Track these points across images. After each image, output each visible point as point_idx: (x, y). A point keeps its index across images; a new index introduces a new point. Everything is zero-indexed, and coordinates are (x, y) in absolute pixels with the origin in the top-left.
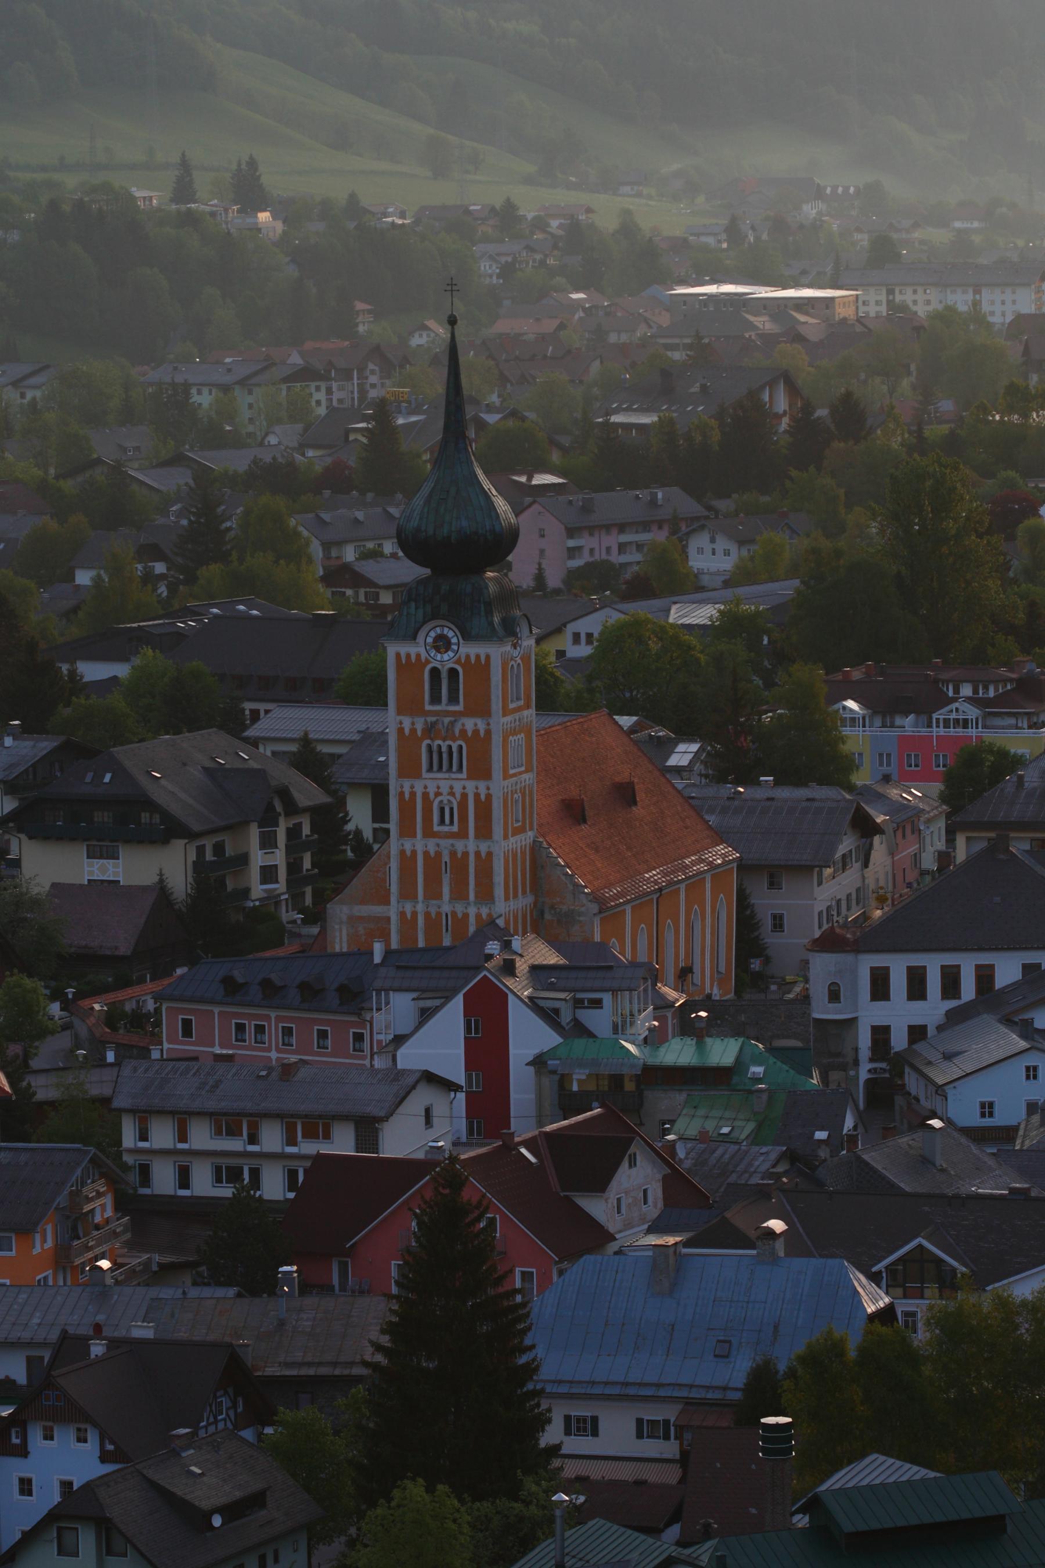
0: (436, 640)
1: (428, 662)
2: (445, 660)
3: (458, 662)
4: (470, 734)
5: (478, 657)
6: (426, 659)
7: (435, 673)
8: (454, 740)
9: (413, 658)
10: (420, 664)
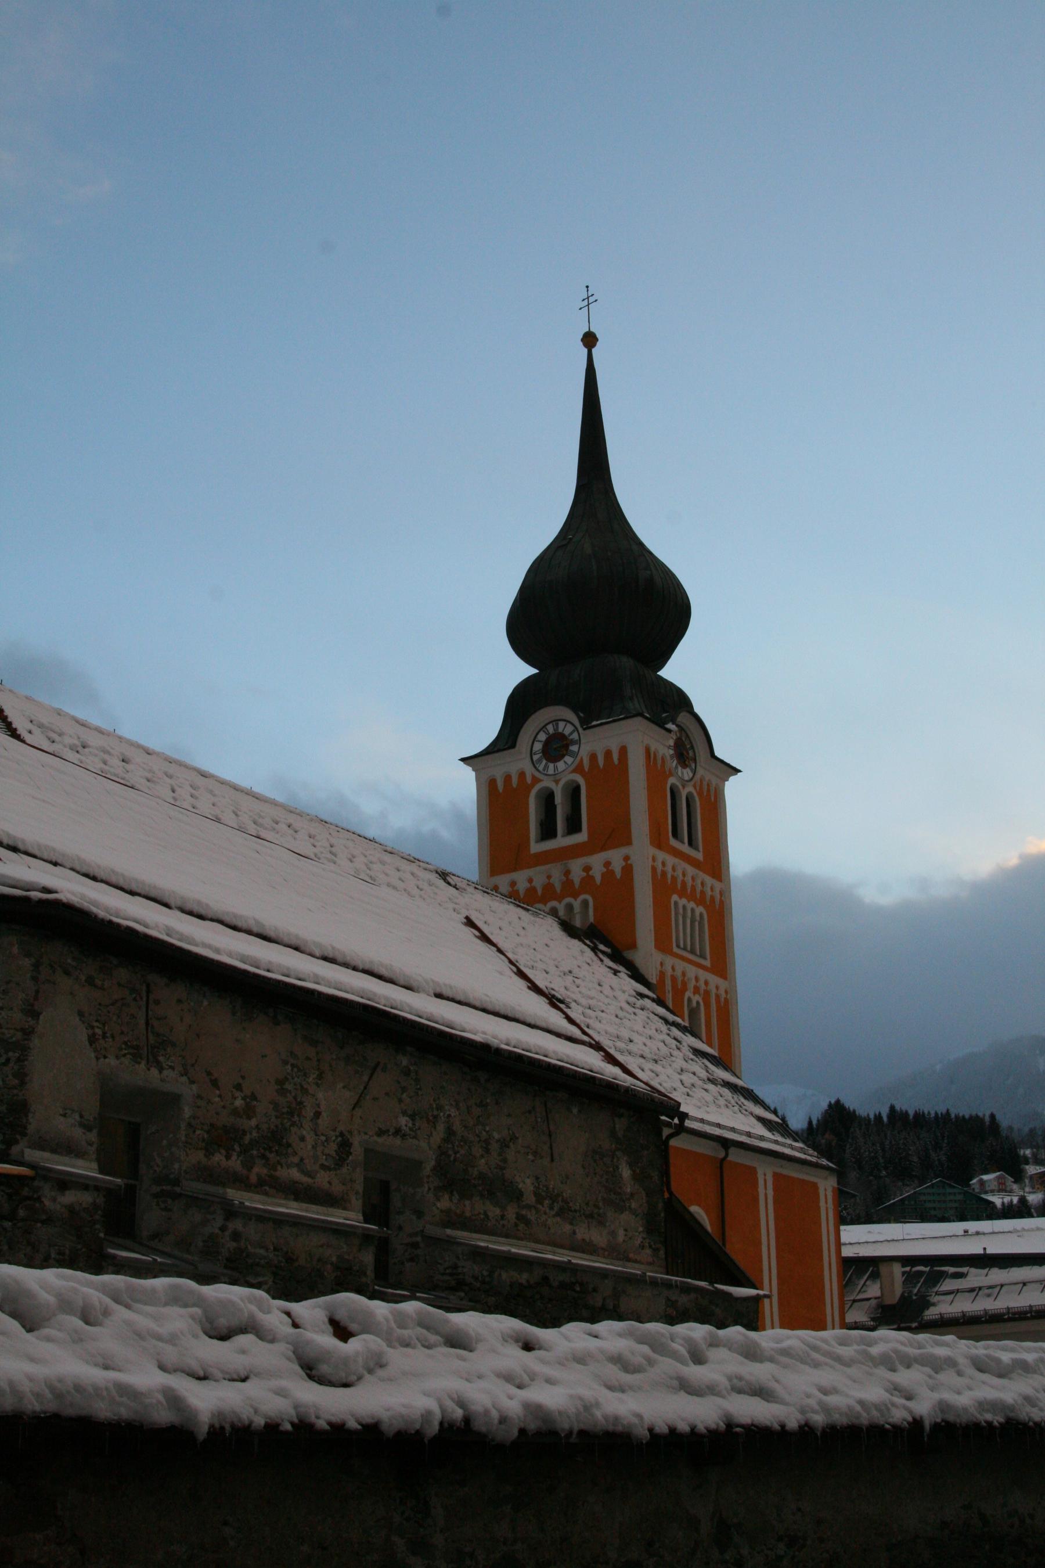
0: (547, 744)
1: (536, 780)
2: (560, 775)
3: (579, 769)
4: (598, 879)
5: (608, 754)
6: (533, 777)
7: (548, 798)
8: (575, 896)
10: (524, 787)
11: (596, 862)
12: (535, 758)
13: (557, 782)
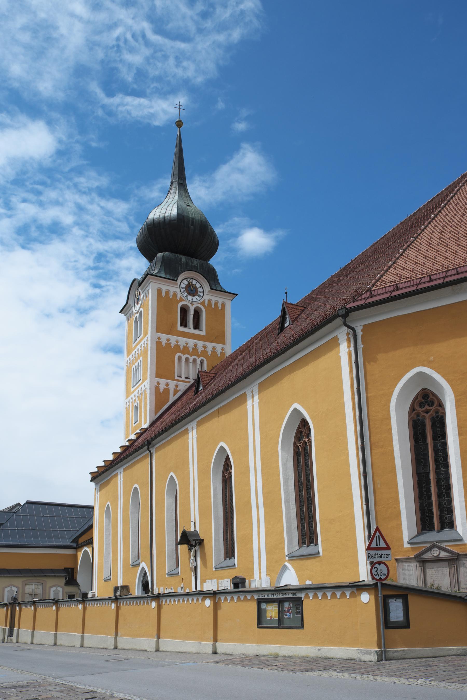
1: (181, 300)
2: (193, 302)
3: (203, 304)
4: (209, 353)
5: (216, 303)
8: (199, 357)
9: (171, 295)
11: (210, 346)
12: (182, 290)
13: (192, 304)
